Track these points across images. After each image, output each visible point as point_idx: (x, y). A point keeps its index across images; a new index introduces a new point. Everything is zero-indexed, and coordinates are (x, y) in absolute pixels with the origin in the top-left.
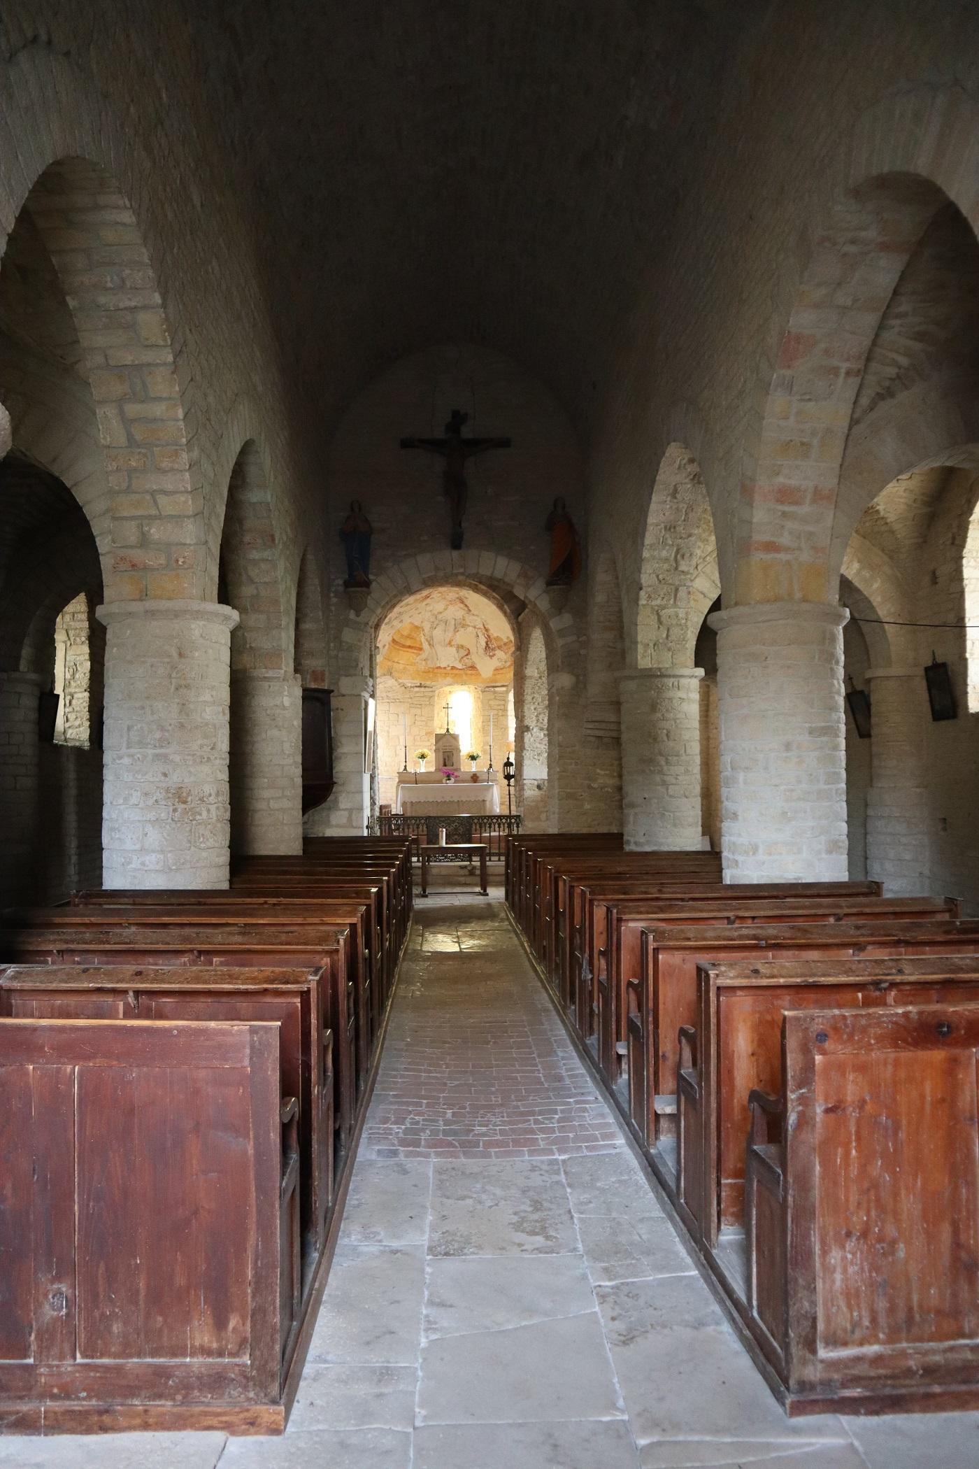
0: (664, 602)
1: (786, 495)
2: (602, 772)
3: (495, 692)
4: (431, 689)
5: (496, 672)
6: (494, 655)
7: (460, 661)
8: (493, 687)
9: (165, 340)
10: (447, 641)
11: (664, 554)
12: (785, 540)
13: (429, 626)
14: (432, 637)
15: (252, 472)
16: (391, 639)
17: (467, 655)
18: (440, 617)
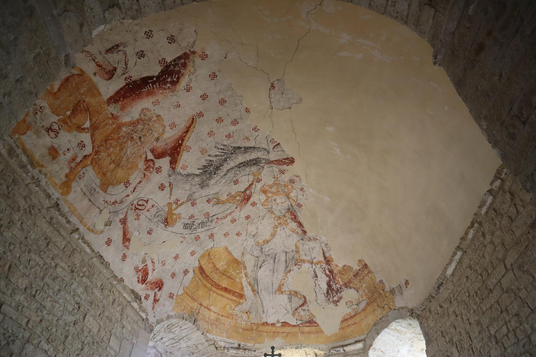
3: (346, 354)
5: (345, 324)
6: (341, 298)
7: (293, 315)
8: (343, 346)
10: (276, 286)
13: (253, 262)
14: (256, 280)
16: (197, 265)
17: (303, 305)
18: (266, 248)
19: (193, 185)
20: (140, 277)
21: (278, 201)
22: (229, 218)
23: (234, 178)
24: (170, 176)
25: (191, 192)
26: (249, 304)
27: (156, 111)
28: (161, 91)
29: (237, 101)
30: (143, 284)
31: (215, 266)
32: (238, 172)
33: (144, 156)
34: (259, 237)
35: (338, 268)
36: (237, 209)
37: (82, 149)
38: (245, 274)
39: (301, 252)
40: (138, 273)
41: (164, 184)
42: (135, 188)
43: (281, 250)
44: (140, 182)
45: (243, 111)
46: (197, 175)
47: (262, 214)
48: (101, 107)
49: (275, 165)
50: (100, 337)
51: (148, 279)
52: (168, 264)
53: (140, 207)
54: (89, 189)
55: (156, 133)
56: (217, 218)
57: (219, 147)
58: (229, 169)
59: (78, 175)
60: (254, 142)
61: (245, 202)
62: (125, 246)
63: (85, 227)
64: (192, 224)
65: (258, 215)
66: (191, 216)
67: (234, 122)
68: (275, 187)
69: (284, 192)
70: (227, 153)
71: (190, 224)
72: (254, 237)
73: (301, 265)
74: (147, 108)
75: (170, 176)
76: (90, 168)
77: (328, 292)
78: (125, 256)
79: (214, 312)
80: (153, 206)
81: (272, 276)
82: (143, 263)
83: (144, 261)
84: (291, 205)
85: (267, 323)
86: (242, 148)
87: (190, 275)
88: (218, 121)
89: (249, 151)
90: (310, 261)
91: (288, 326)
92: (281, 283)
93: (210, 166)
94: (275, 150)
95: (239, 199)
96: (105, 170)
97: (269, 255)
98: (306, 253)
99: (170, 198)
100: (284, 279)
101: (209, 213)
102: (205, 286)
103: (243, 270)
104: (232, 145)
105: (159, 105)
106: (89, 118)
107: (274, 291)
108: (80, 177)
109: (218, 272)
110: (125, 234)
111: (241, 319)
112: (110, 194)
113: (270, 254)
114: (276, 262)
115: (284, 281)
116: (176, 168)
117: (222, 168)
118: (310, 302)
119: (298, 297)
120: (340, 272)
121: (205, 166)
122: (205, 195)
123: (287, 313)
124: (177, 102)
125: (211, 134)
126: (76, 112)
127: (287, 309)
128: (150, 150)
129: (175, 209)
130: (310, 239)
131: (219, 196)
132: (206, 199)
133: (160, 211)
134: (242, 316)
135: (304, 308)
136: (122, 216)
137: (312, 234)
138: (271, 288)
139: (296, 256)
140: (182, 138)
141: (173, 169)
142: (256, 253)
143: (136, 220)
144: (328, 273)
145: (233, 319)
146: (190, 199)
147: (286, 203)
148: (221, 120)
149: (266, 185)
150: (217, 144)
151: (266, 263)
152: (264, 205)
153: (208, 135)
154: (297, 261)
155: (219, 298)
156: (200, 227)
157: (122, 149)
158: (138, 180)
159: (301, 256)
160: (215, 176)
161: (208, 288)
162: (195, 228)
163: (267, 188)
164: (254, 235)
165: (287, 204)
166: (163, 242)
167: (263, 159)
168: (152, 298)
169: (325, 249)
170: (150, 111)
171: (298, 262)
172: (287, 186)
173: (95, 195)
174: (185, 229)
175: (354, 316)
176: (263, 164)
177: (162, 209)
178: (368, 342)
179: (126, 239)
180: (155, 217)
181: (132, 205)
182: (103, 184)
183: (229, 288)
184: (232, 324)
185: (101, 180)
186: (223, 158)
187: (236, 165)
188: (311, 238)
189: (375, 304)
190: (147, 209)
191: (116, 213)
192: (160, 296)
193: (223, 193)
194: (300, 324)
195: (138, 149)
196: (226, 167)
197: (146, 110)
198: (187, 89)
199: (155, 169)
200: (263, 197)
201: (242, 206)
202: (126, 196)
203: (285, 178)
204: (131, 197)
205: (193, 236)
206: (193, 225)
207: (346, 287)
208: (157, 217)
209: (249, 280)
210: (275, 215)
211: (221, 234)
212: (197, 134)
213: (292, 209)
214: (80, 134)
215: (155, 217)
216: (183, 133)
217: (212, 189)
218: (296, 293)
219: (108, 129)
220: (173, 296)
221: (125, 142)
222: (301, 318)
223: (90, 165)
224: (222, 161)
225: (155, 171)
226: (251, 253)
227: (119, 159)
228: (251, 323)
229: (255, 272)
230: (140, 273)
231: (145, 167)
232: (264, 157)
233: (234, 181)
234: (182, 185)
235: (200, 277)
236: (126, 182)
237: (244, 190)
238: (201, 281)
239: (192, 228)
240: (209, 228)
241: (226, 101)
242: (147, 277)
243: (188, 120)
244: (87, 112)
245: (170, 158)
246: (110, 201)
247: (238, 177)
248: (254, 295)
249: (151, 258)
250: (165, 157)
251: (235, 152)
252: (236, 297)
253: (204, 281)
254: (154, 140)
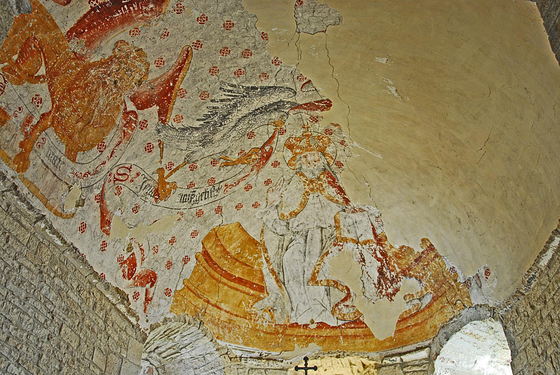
3: (403, 365)
4: (280, 365)
6: (397, 290)
8: (400, 354)
10: (308, 275)
14: (280, 266)
16: (201, 250)
18: (294, 222)
19: (191, 142)
20: (126, 270)
21: (309, 158)
22: (242, 184)
23: (247, 131)
24: (159, 131)
25: (189, 152)
26: (272, 298)
27: (136, 44)
28: (141, 15)
29: (249, 24)
30: (129, 279)
31: (225, 250)
32: (253, 122)
33: (122, 107)
34: (283, 209)
35: (393, 250)
36: (253, 172)
37: (38, 106)
38: (265, 258)
39: (341, 227)
40: (123, 266)
41: (152, 144)
42: (113, 152)
43: (315, 225)
44: (120, 142)
45: (258, 37)
46: (197, 129)
47: (287, 177)
48: (59, 44)
49: (305, 111)
50: (81, 352)
51: (136, 272)
52: (162, 250)
53: (121, 178)
54: (52, 159)
55: (138, 74)
56: (226, 186)
57: (225, 88)
58: (241, 117)
59: (37, 142)
60: (274, 81)
61: (264, 161)
62: (104, 231)
63: (51, 211)
64: (192, 195)
65: (282, 179)
66: (190, 185)
67: (246, 52)
68: (305, 140)
69: (318, 147)
70: (236, 96)
71: (189, 195)
72: (277, 208)
73: (342, 245)
74: (122, 40)
75: (159, 131)
76: (50, 131)
77: (379, 282)
78: (105, 244)
79: (225, 311)
80: (138, 174)
81: (303, 261)
82: (128, 252)
83: (130, 248)
84: (328, 164)
85: (297, 323)
86: (257, 89)
87: (192, 263)
88: (223, 53)
89: (268, 92)
90: (355, 240)
91: (326, 328)
92: (315, 269)
93: (213, 115)
94: (304, 90)
95: (255, 158)
96: (71, 131)
97: (298, 232)
98: (349, 228)
99: (161, 162)
100: (319, 265)
101: (214, 178)
102: (213, 277)
103: (262, 254)
104: (244, 85)
105: (140, 34)
106: (43, 62)
107: (306, 281)
108: (39, 144)
109: (229, 257)
110: (103, 216)
111: (262, 319)
112: (80, 164)
113: (299, 231)
114: (307, 242)
115: (319, 266)
116: (167, 120)
117: (230, 117)
118: (355, 295)
119: (338, 289)
120: (396, 255)
121: (207, 115)
122: (209, 155)
123: (324, 310)
124: (165, 29)
125: (213, 71)
126: (26, 55)
127: (324, 305)
128: (130, 98)
129: (168, 176)
130: (354, 211)
131: (228, 155)
132: (210, 160)
133: (148, 180)
134: (262, 315)
135: (347, 303)
136: (97, 192)
137: (358, 204)
138: (302, 277)
139: (335, 233)
140: (174, 79)
141: (164, 122)
142: (281, 229)
143: (116, 195)
144: (379, 256)
145: (251, 319)
146: (188, 161)
147: (321, 162)
148: (227, 51)
149: (292, 138)
150: (223, 85)
151: (294, 242)
152: (290, 165)
153: (210, 72)
154: (337, 240)
155: (232, 292)
156: (203, 198)
157: (93, 100)
158: (117, 140)
159: (342, 233)
160: (221, 128)
161: (217, 280)
162: (196, 201)
163: (294, 141)
164: (277, 206)
165: (322, 162)
166: (154, 222)
167: (288, 102)
168: (142, 297)
169: (376, 224)
170: (128, 43)
171: (339, 241)
172: (321, 139)
173: (60, 167)
174: (183, 202)
175: (415, 314)
176: (287, 109)
177: (151, 177)
178: (434, 349)
179: (105, 222)
180: (141, 188)
181: (110, 175)
182: (69, 150)
183: (246, 278)
184: (250, 327)
185: (67, 146)
186: (232, 103)
187: (250, 111)
188: (355, 208)
189: (444, 300)
190: (130, 179)
191: (89, 188)
192: (153, 294)
193: (233, 152)
194: (342, 325)
195: (114, 98)
196: (236, 115)
197: (121, 43)
198: (178, 10)
199: (138, 124)
200: (289, 154)
201: (259, 167)
202: (102, 164)
203: (320, 127)
204: (108, 165)
205: (194, 211)
206: (193, 197)
207: (405, 275)
208: (145, 188)
209: (271, 267)
210: (305, 178)
211: (232, 206)
212: (194, 71)
213: (329, 170)
214: (33, 85)
215: (141, 188)
216: (175, 72)
217: (218, 146)
218: (336, 283)
219: (71, 75)
220: (170, 293)
221: (96, 90)
222: (343, 317)
223: (50, 126)
224: (231, 107)
225: (139, 126)
226: (274, 230)
227: (89, 114)
228: (276, 325)
229: (279, 256)
230: (126, 265)
231: (125, 122)
232: (290, 100)
233: (248, 134)
234: (177, 144)
235: (206, 264)
236: (101, 145)
237: (261, 145)
238: (207, 271)
239: (193, 200)
240: (216, 200)
241: (233, 24)
242: (134, 269)
243: (180, 54)
244: (40, 54)
245: (158, 108)
246: (81, 173)
247: (254, 129)
248: (279, 286)
249: (139, 244)
250: (151, 107)
251: (249, 94)
252: (254, 289)
253: (210, 270)
254: (135, 84)
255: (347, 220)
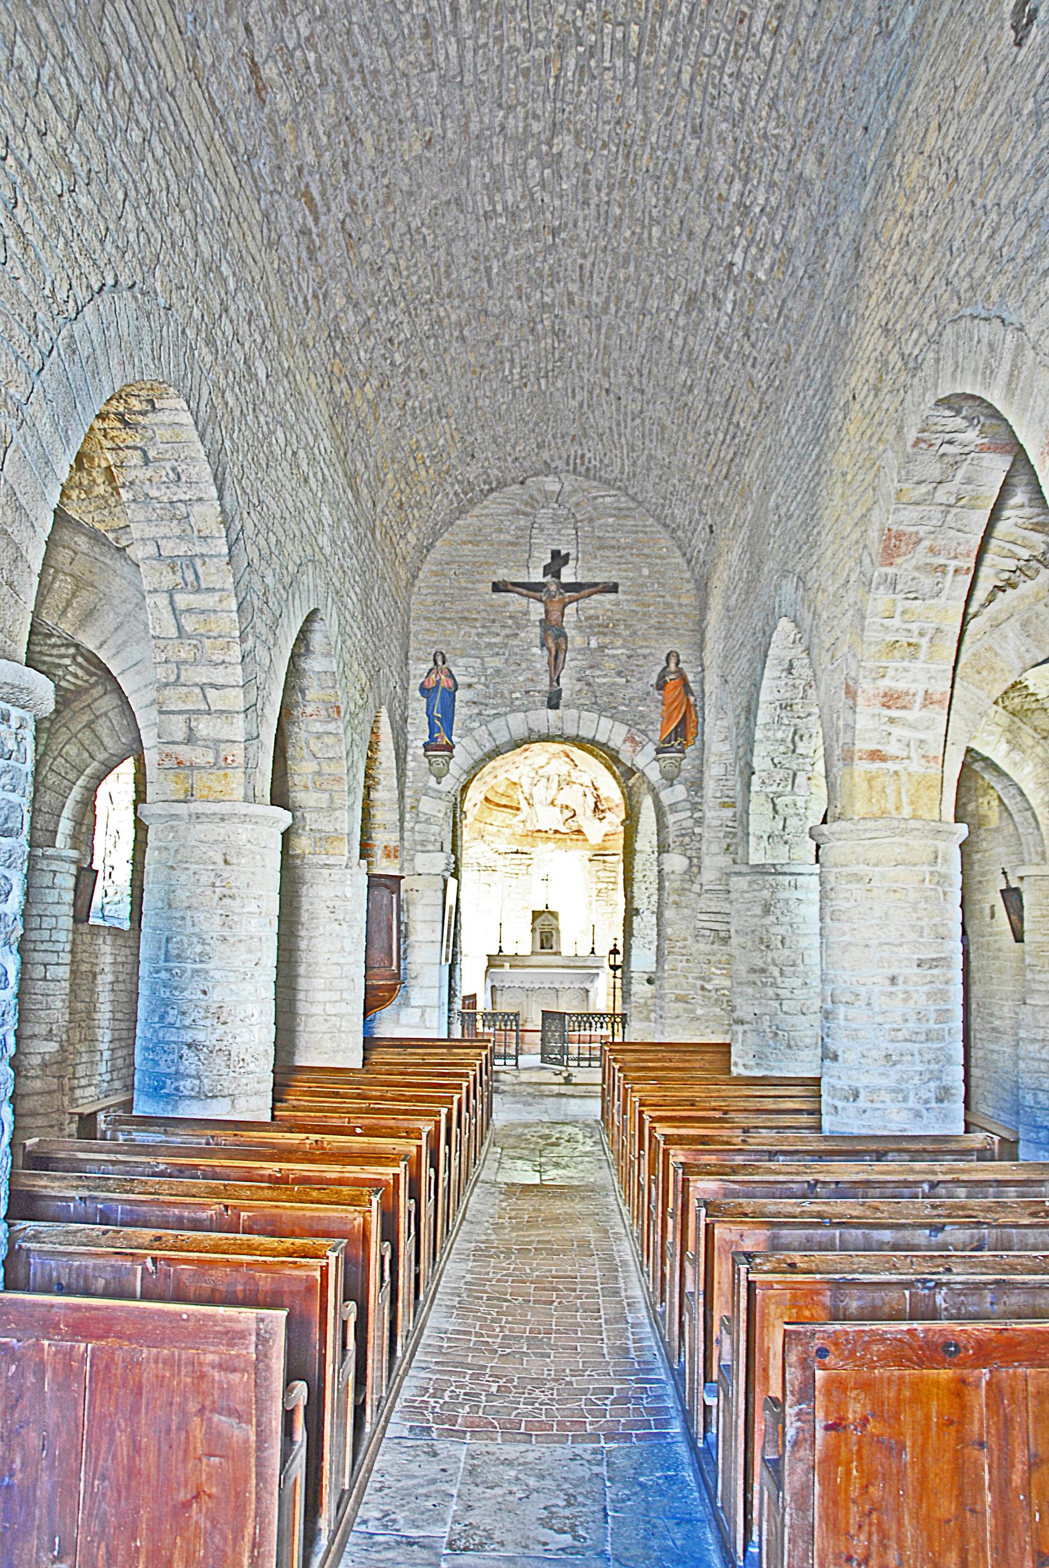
0: (780, 789)
1: (891, 699)
2: (719, 972)
9: (219, 531)
11: (780, 735)
12: (892, 748)
14: (531, 795)
15: (317, 639)
18: (541, 772)
142: (533, 774)
255: (575, 774)
